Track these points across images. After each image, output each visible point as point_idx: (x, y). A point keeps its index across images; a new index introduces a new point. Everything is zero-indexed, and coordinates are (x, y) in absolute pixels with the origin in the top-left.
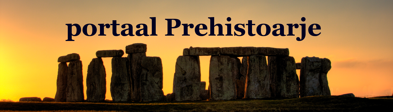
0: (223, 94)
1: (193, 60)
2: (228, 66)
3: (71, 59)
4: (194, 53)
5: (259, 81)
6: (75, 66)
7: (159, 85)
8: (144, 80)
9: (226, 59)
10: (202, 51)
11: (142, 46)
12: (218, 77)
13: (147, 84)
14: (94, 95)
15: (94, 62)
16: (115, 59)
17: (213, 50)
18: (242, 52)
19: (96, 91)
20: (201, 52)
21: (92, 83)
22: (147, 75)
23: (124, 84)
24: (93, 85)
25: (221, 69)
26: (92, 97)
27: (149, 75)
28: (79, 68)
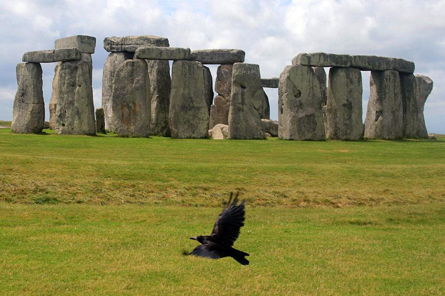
0: (352, 130)
1: (311, 74)
2: (359, 85)
3: (70, 58)
4: (317, 63)
5: (394, 112)
6: (80, 71)
7: (260, 112)
8: (239, 103)
11: (164, 41)
16: (183, 64)
17: (342, 58)
18: (377, 64)
20: (327, 61)
21: (128, 104)
23: (199, 108)
24: (129, 108)
25: (349, 90)
28: (88, 75)
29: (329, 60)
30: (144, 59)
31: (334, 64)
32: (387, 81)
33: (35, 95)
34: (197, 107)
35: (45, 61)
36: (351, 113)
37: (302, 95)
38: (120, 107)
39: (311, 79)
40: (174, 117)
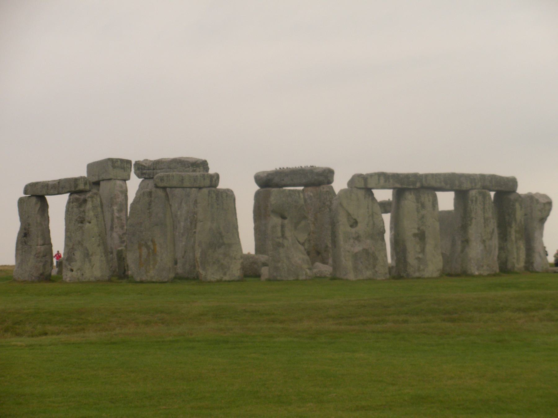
2: (434, 209)
6: (89, 205)
7: (306, 247)
8: (278, 238)
10: (391, 181)
12: (416, 231)
13: (285, 245)
14: (151, 266)
15: (151, 197)
16: (209, 192)
18: (457, 183)
19: (159, 259)
20: (389, 181)
21: (146, 243)
22: (283, 226)
23: (230, 246)
24: (148, 247)
28: (99, 209)
30: (164, 188)
31: (398, 186)
32: (472, 202)
37: (359, 225)
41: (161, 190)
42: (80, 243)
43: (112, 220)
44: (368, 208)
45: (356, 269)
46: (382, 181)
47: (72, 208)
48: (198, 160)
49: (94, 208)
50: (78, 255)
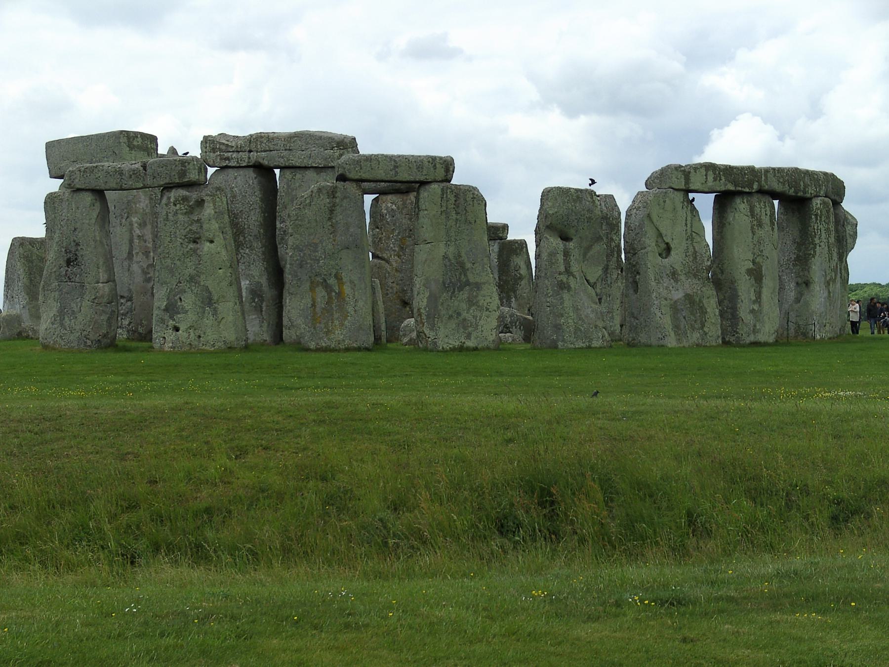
6: (209, 210)
7: (598, 291)
9: (768, 209)
12: (751, 266)
14: (337, 323)
19: (350, 309)
21: (325, 281)
23: (478, 286)
26: (328, 332)
27: (576, 254)
29: (723, 178)
32: (817, 219)
33: (101, 263)
34: (476, 283)
35: (124, 186)
36: (761, 287)
37: (672, 253)
38: (308, 285)
39: (689, 218)
40: (427, 306)
41: (354, 185)
42: (192, 279)
43: (131, 241)
44: (686, 225)
45: (676, 327)
46: (711, 178)
47: (176, 213)
48: (346, 137)
49: (218, 215)
50: (189, 301)
